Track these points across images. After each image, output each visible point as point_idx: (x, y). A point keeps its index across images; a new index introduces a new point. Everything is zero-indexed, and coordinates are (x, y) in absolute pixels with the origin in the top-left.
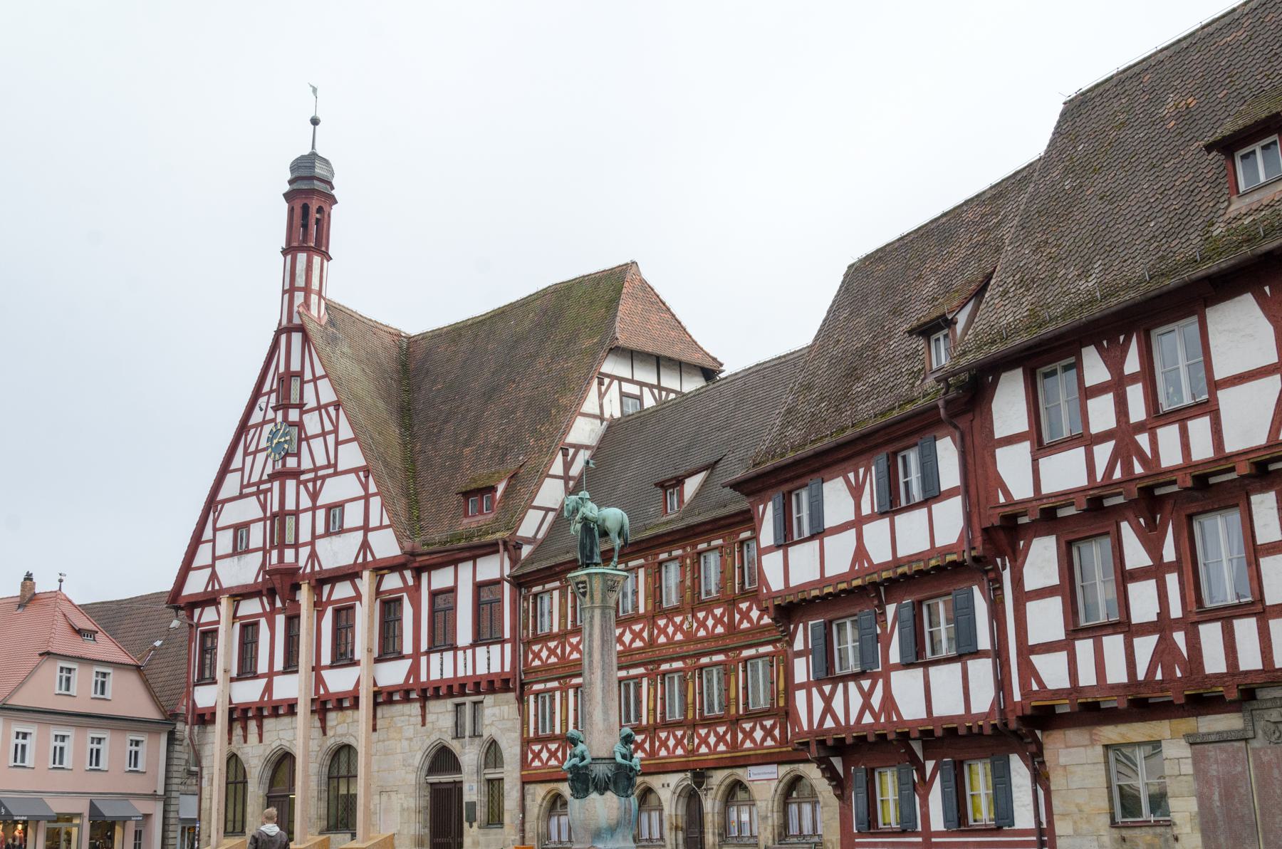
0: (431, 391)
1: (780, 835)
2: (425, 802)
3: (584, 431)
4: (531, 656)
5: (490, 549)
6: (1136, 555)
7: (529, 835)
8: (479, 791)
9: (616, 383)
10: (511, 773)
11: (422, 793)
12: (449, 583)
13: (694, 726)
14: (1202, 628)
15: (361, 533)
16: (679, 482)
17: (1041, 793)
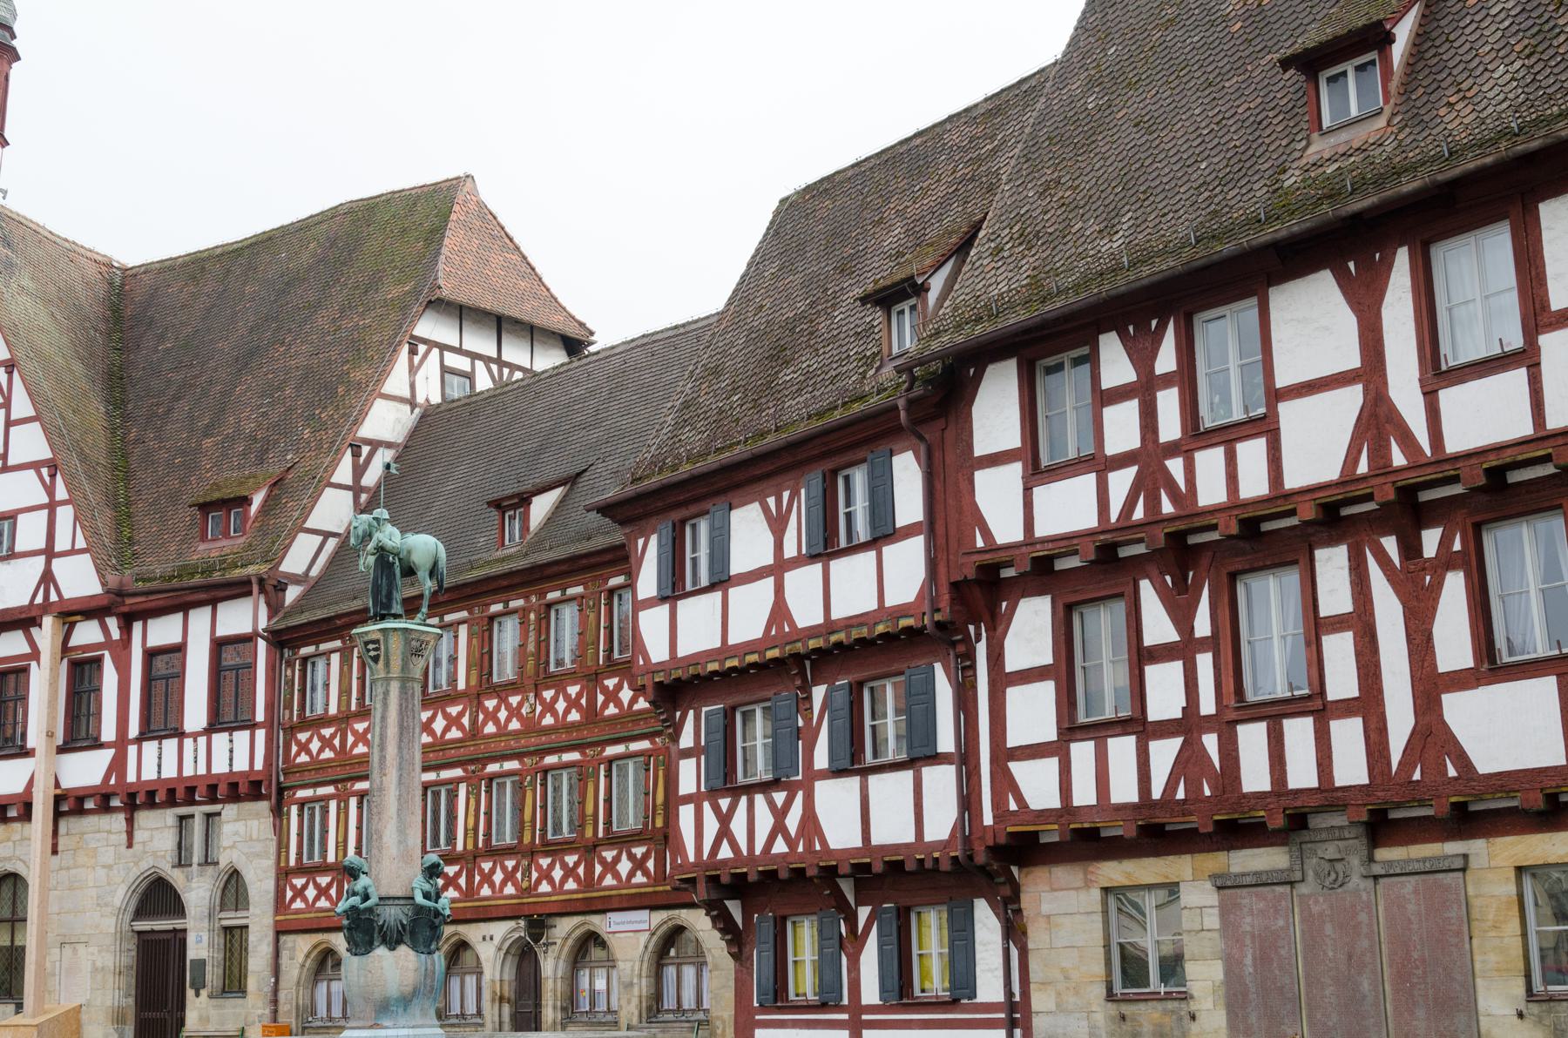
0: (157, 351)
1: (649, 1009)
2: (129, 958)
3: (386, 421)
4: (294, 749)
5: (239, 589)
6: (1158, 627)
7: (283, 1007)
8: (211, 945)
9: (435, 351)
10: (259, 919)
11: (125, 946)
12: (174, 638)
13: (532, 853)
14: (1240, 729)
15: (42, 559)
16: (524, 500)
17: (1014, 953)
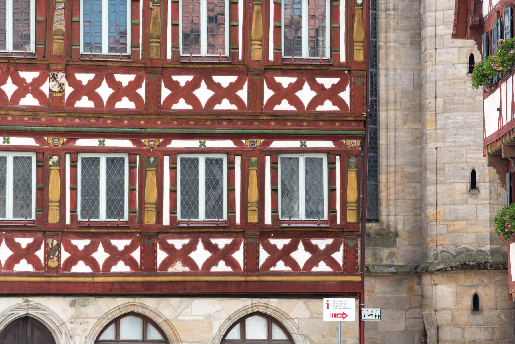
13: (63, 233)
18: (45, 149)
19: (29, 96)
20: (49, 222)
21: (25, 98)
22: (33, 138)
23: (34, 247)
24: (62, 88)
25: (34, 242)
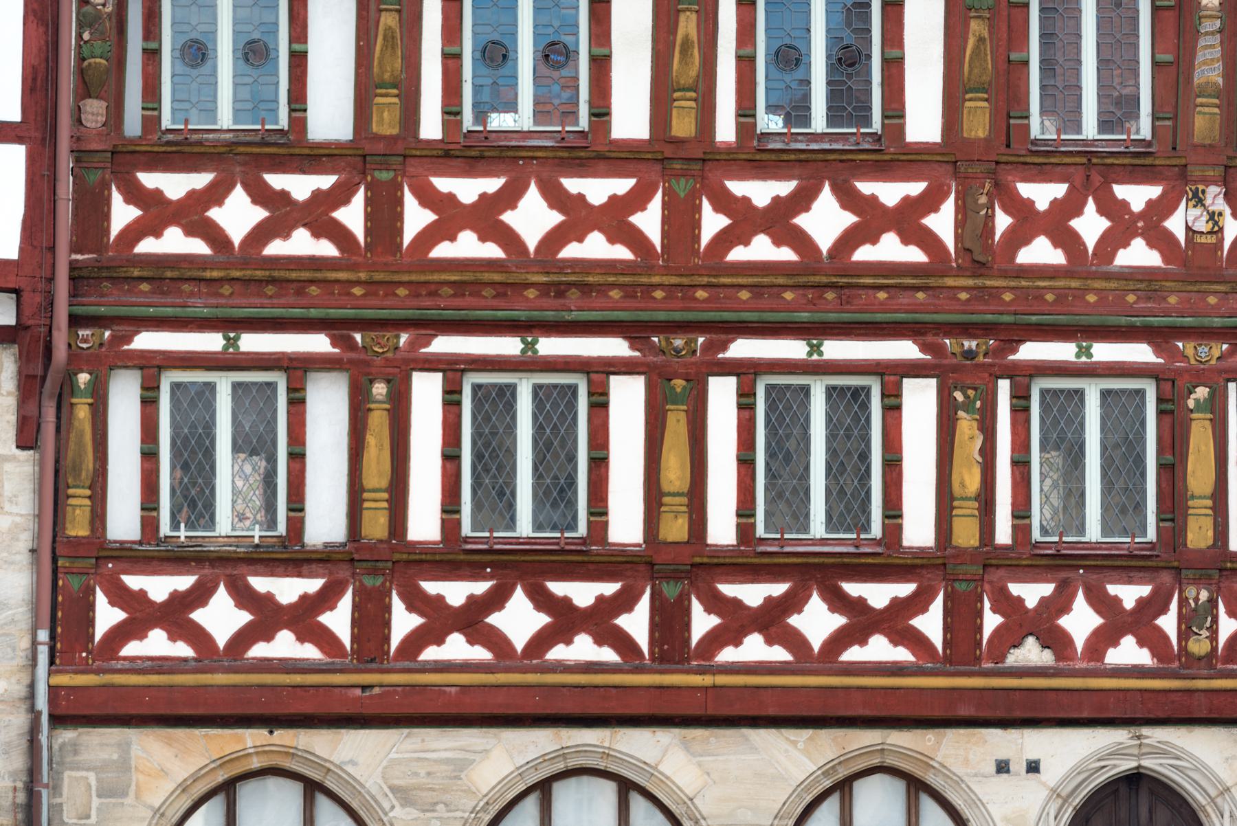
4: (122, 214)
18: (1179, 372)
19: (1138, 244)
20: (1189, 545)
21: (1129, 249)
22: (1149, 343)
23: (1153, 606)
24: (1216, 223)
25: (1154, 594)
